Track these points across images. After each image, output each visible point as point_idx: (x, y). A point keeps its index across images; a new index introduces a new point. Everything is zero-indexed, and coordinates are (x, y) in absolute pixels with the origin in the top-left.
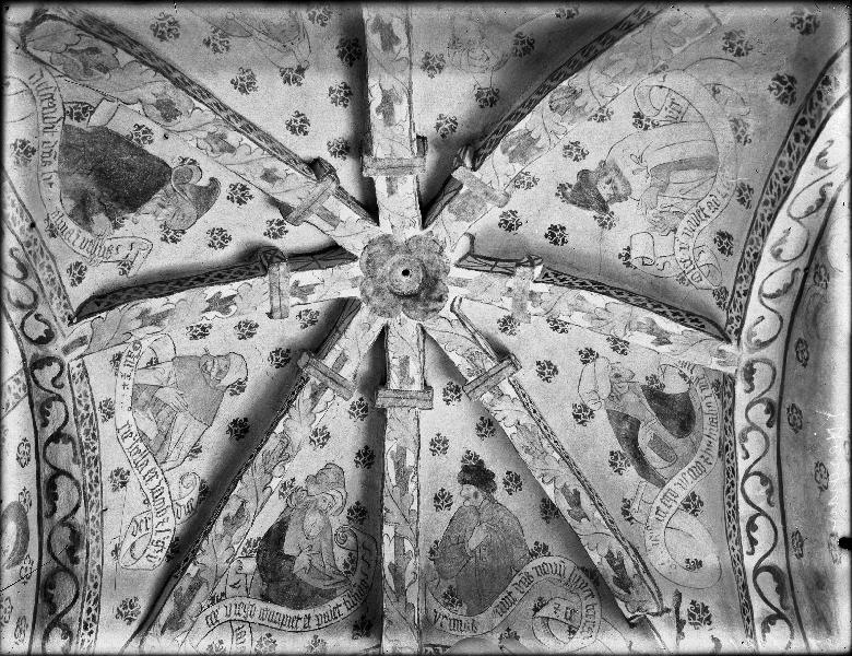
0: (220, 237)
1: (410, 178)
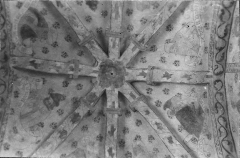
0: (166, 91)
1: (108, 107)
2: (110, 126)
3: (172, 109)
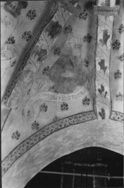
2: (102, 33)
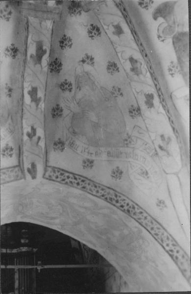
3: (171, 23)
